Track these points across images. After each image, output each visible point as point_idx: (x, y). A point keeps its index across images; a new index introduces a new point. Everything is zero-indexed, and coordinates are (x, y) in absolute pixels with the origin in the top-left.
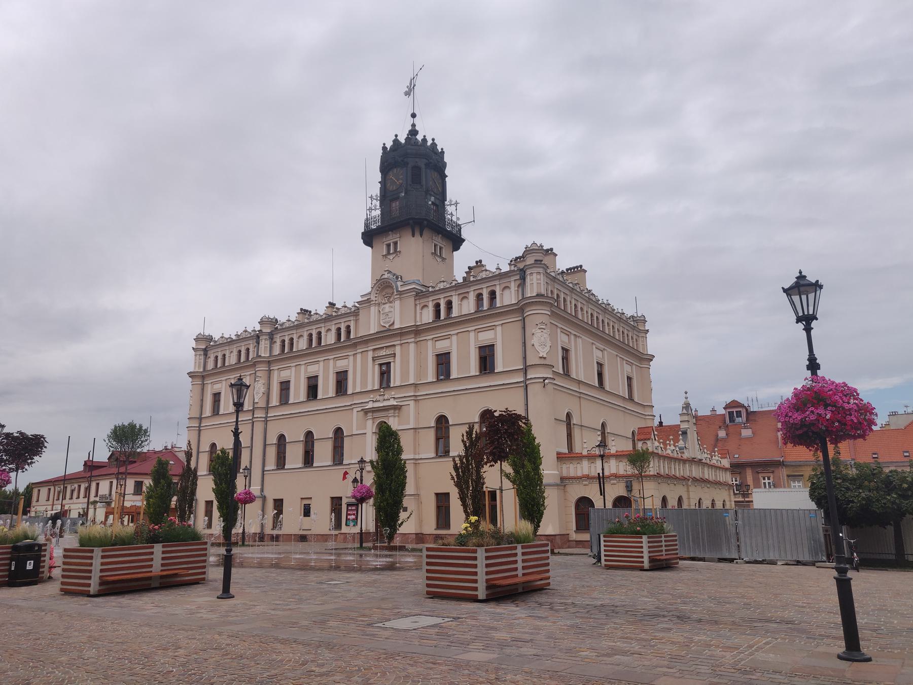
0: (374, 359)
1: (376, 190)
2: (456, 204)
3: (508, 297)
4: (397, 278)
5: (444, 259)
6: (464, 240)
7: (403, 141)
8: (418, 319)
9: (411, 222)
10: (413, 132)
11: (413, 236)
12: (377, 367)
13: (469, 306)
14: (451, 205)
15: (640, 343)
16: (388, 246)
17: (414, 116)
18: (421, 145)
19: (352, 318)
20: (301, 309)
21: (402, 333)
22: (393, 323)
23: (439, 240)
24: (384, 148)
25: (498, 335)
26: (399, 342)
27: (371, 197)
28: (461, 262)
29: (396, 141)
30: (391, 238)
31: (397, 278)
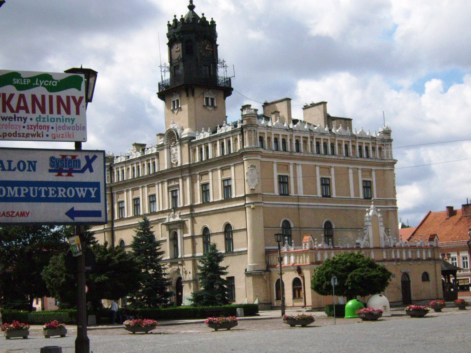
0: (169, 188)
5: (215, 108)
7: (179, 20)
9: (183, 87)
10: (191, 7)
11: (188, 96)
12: (170, 193)
15: (385, 151)
16: (174, 102)
21: (182, 169)
23: (209, 95)
24: (169, 25)
29: (175, 20)
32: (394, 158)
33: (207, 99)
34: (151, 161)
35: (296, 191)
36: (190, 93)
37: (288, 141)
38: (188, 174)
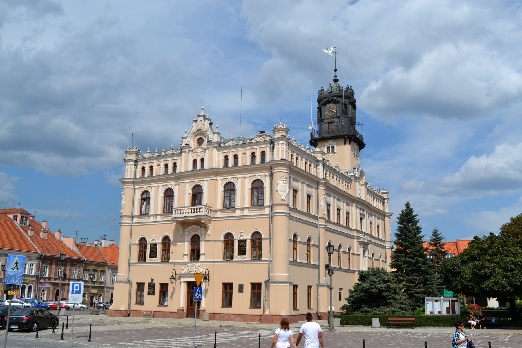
10: (336, 81)
14: (359, 125)
16: (328, 148)
17: (336, 70)
23: (355, 145)
24: (322, 90)
30: (331, 143)
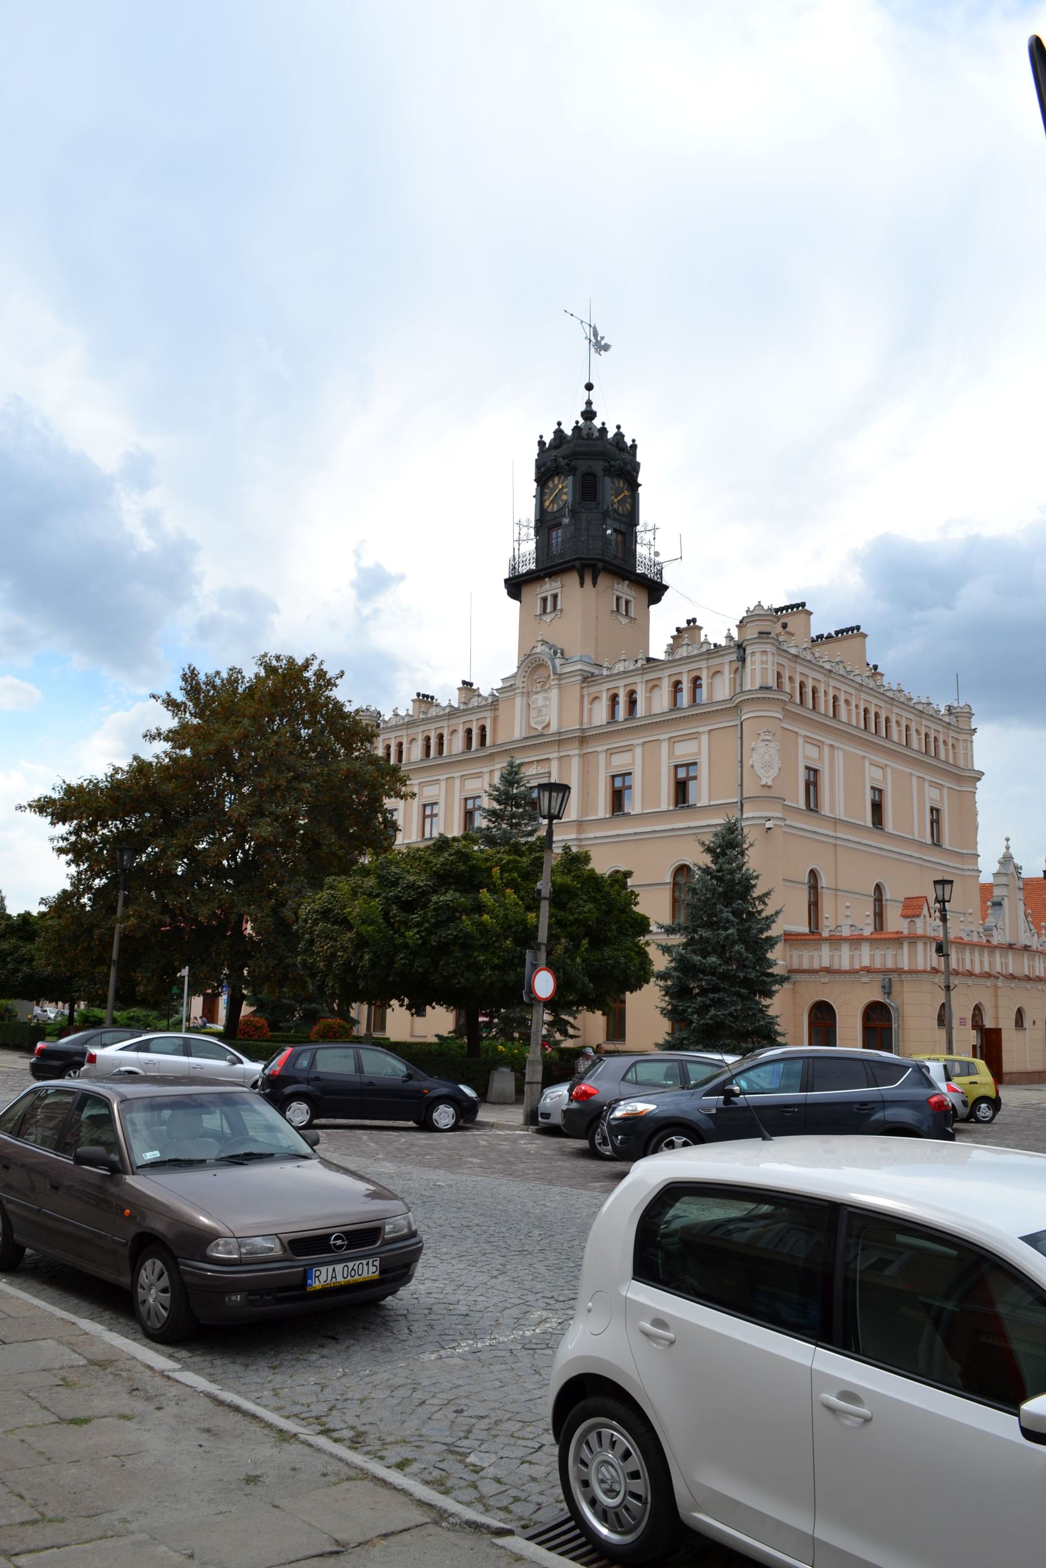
1: (528, 511)
2: (655, 529)
3: (721, 690)
4: (555, 653)
6: (666, 588)
7: (568, 432)
8: (586, 719)
10: (589, 414)
11: (582, 584)
13: (662, 701)
14: (646, 531)
15: (960, 751)
16: (545, 600)
17: (589, 387)
18: (597, 439)
19: (488, 714)
20: (418, 694)
22: (548, 725)
23: (625, 590)
24: (541, 443)
25: (697, 748)
26: (556, 755)
27: (519, 524)
28: (662, 624)
29: (559, 433)
30: (549, 587)
31: (555, 653)
32: (977, 767)
33: (618, 599)
34: (475, 723)
35: (832, 809)
36: (588, 581)
37: (821, 694)
38: (577, 752)
